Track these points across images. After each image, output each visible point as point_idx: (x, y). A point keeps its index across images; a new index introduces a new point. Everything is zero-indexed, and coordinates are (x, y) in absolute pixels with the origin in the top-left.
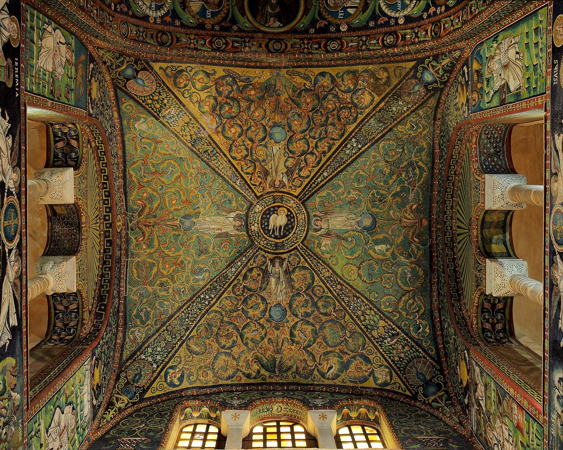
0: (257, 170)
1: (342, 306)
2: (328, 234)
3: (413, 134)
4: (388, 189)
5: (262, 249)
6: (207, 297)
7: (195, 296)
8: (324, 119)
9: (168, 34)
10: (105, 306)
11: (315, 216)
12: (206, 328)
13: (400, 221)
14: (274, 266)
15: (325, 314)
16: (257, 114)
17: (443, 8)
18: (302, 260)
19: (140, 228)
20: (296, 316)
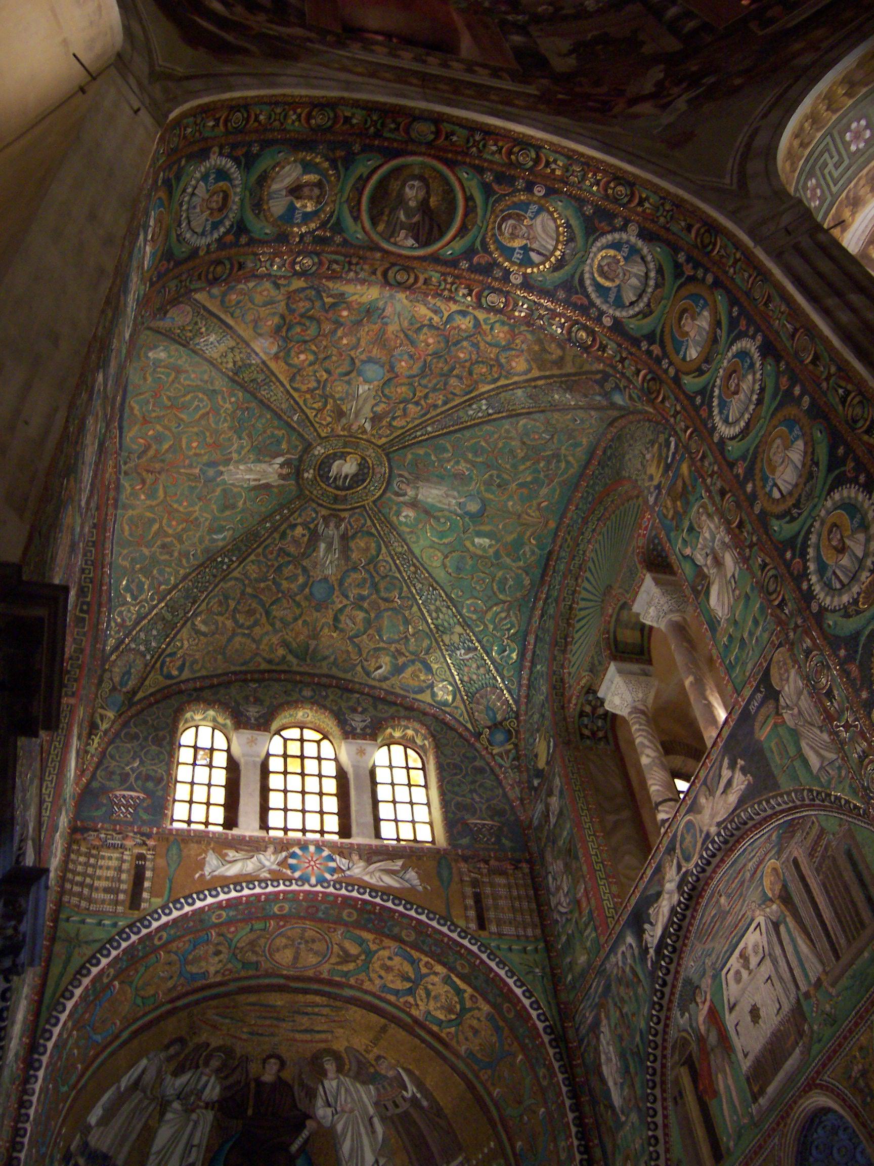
0: (328, 407)
1: (411, 593)
2: (414, 504)
3: (571, 426)
4: (515, 475)
5: (313, 501)
6: (226, 560)
7: (210, 559)
8: (446, 369)
9: (227, 262)
10: (88, 604)
11: (401, 476)
12: (220, 601)
13: (519, 516)
14: (327, 526)
15: (386, 600)
16: (345, 341)
17: (672, 371)
18: (369, 523)
19: (139, 474)
20: (347, 597)
